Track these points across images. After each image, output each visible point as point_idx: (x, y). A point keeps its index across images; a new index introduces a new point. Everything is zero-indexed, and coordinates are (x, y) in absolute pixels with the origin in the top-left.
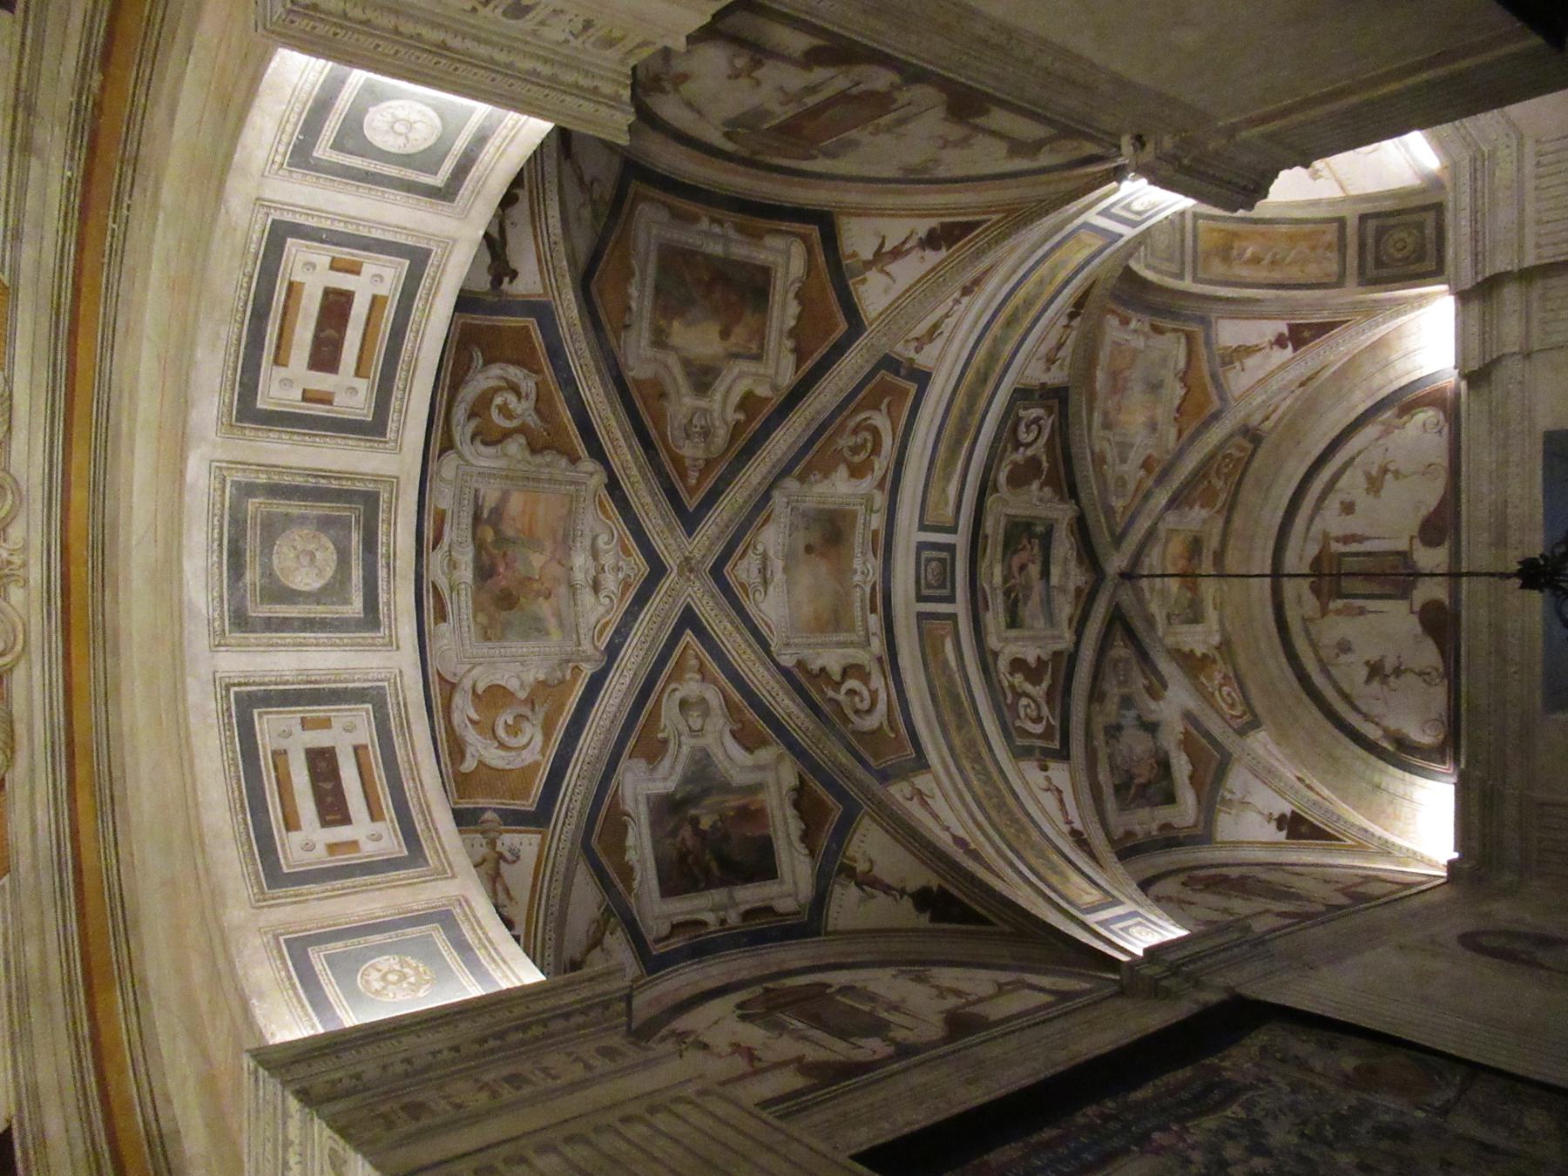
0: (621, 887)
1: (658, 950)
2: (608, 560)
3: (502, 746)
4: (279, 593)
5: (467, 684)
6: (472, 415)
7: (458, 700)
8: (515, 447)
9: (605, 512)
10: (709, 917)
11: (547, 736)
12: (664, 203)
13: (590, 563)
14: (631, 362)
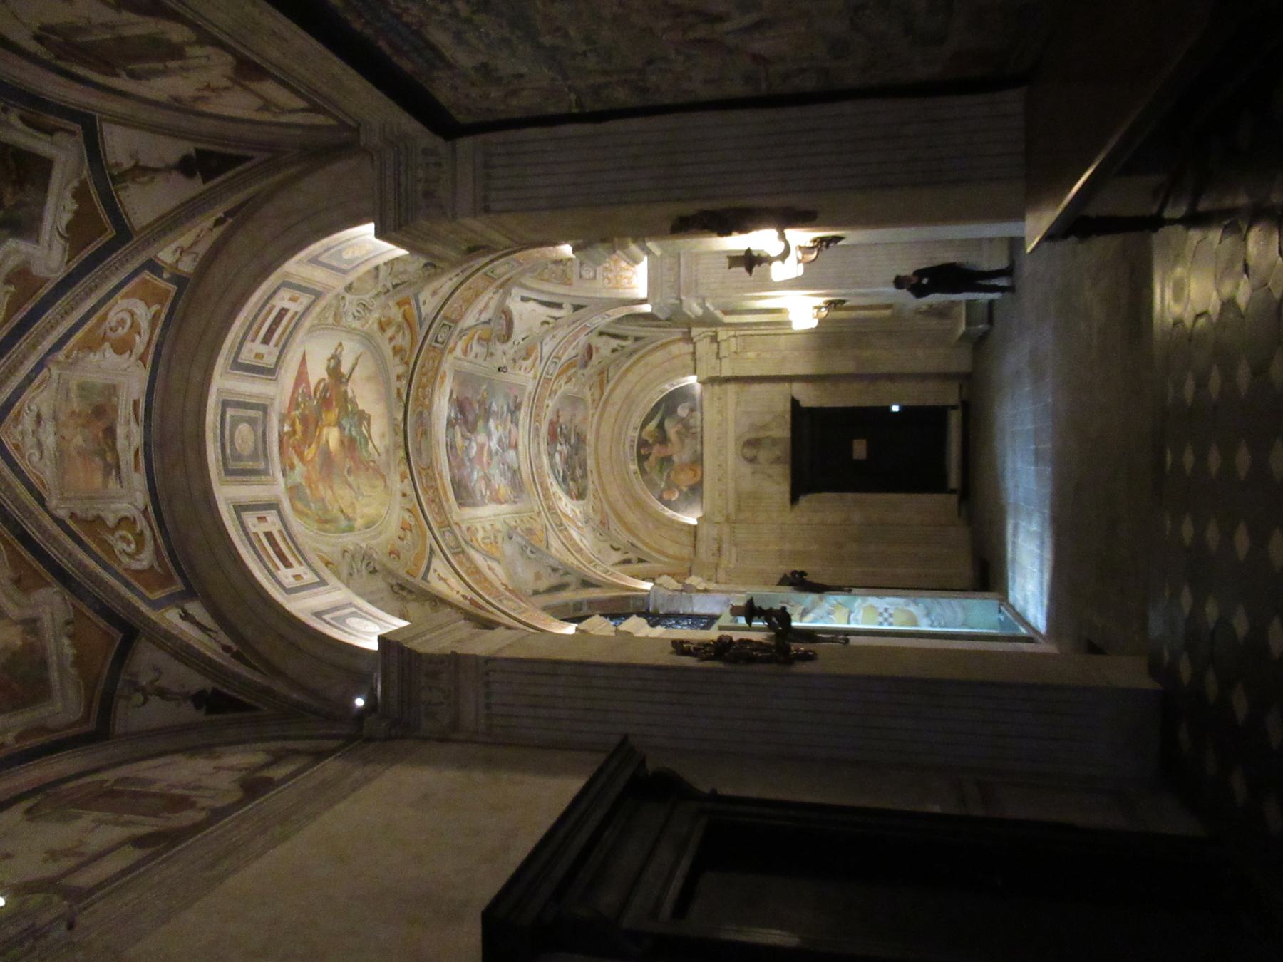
0: (93, 190)
1: (77, 127)
2: (30, 440)
3: (132, 314)
4: (252, 422)
5: (133, 358)
6: (141, 534)
7: (142, 350)
8: (111, 520)
9: (38, 477)
10: (14, 119)
11: (106, 314)
12: (53, 731)
13: (43, 438)
14: (58, 599)
